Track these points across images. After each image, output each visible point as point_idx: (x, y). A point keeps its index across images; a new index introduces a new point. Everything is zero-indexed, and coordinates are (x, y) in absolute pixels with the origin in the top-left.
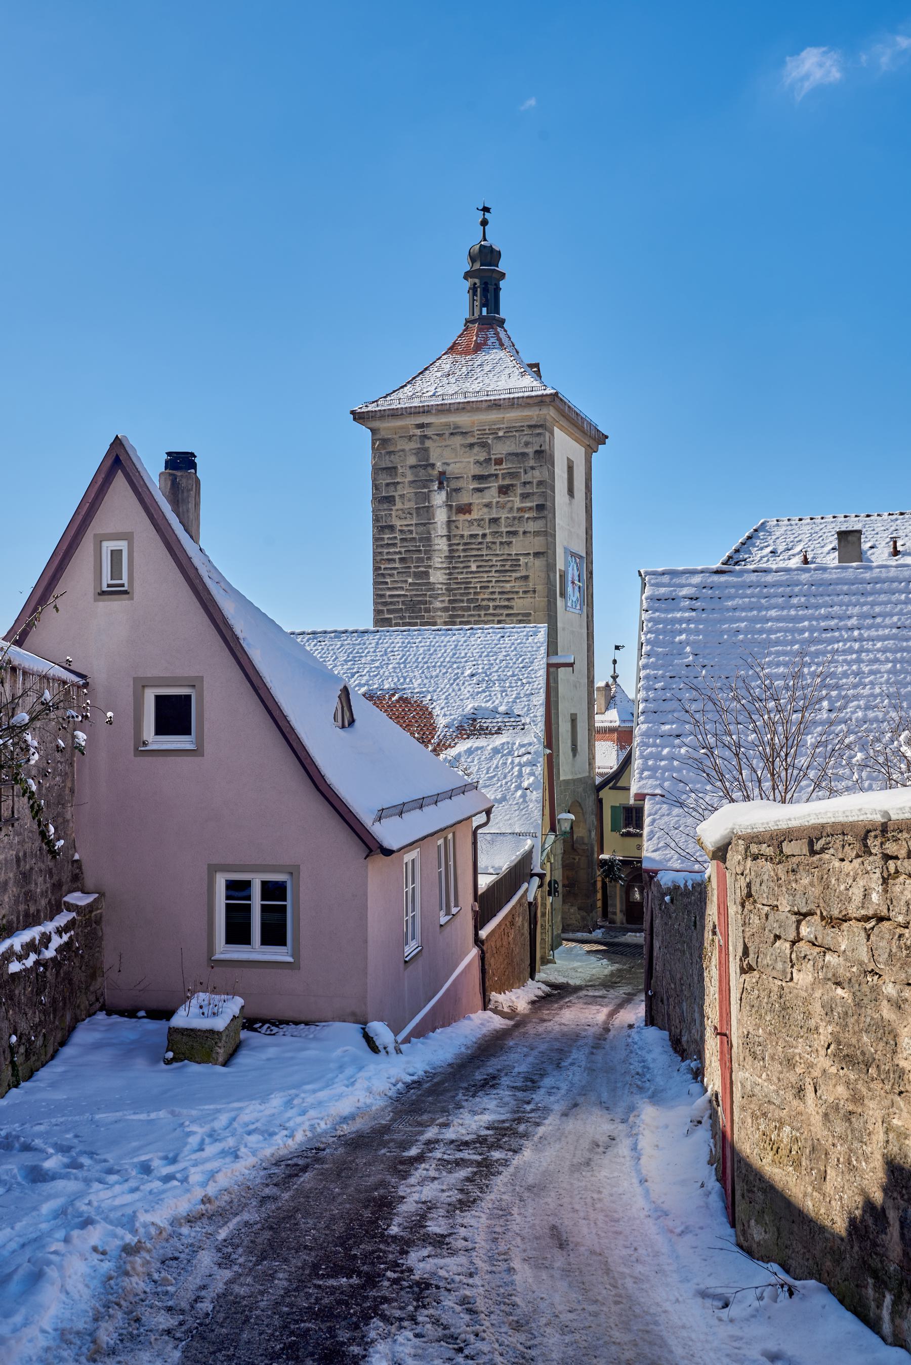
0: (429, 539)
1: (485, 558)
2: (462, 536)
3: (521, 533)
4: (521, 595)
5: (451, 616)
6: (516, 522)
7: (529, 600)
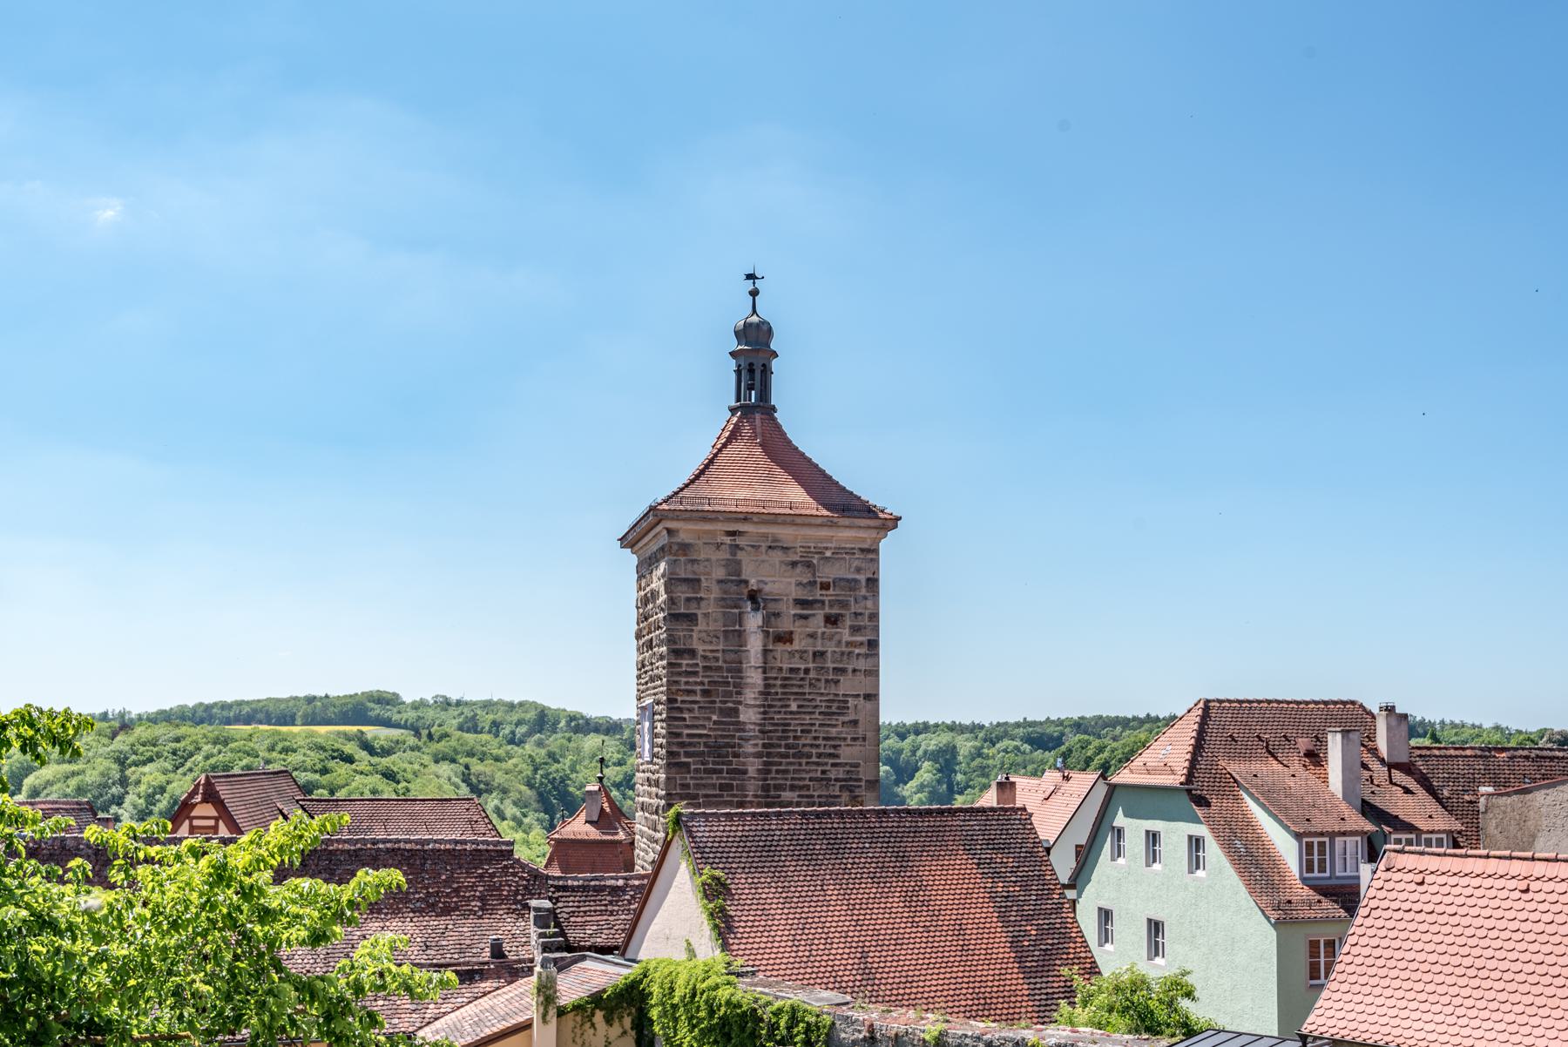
0: (740, 670)
5: (765, 763)
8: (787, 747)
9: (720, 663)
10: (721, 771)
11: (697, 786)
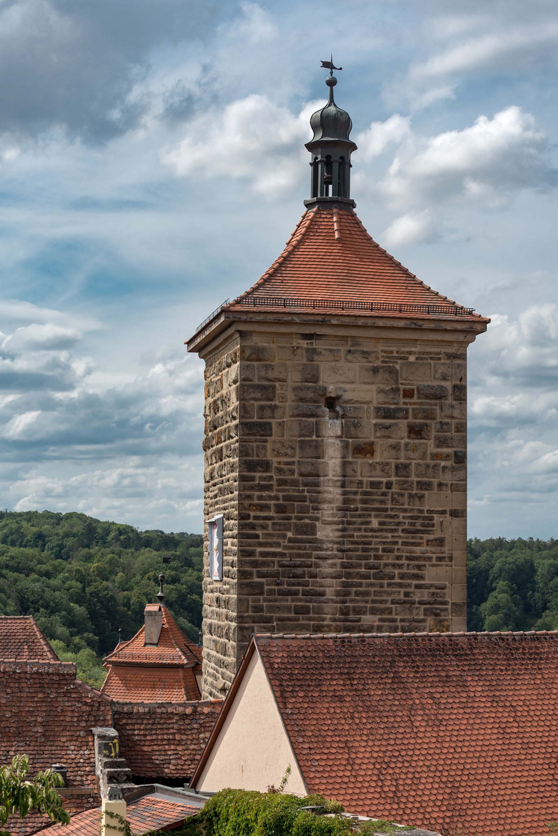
1: (389, 512)
2: (361, 483)
3: (435, 485)
4: (434, 562)
6: (430, 470)
7: (444, 568)
8: (368, 567)
9: (296, 476)
10: (296, 593)
11: (271, 609)
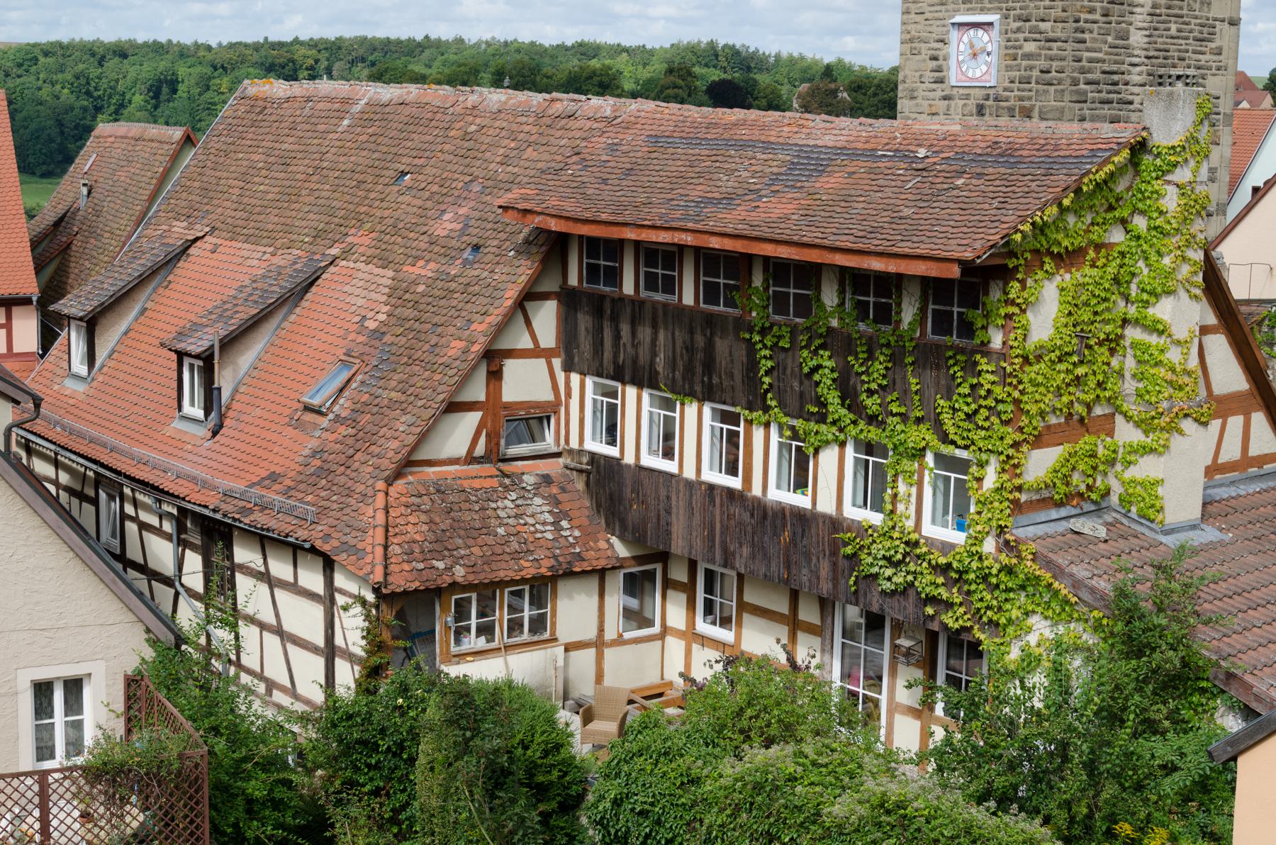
4: (1214, 71)
